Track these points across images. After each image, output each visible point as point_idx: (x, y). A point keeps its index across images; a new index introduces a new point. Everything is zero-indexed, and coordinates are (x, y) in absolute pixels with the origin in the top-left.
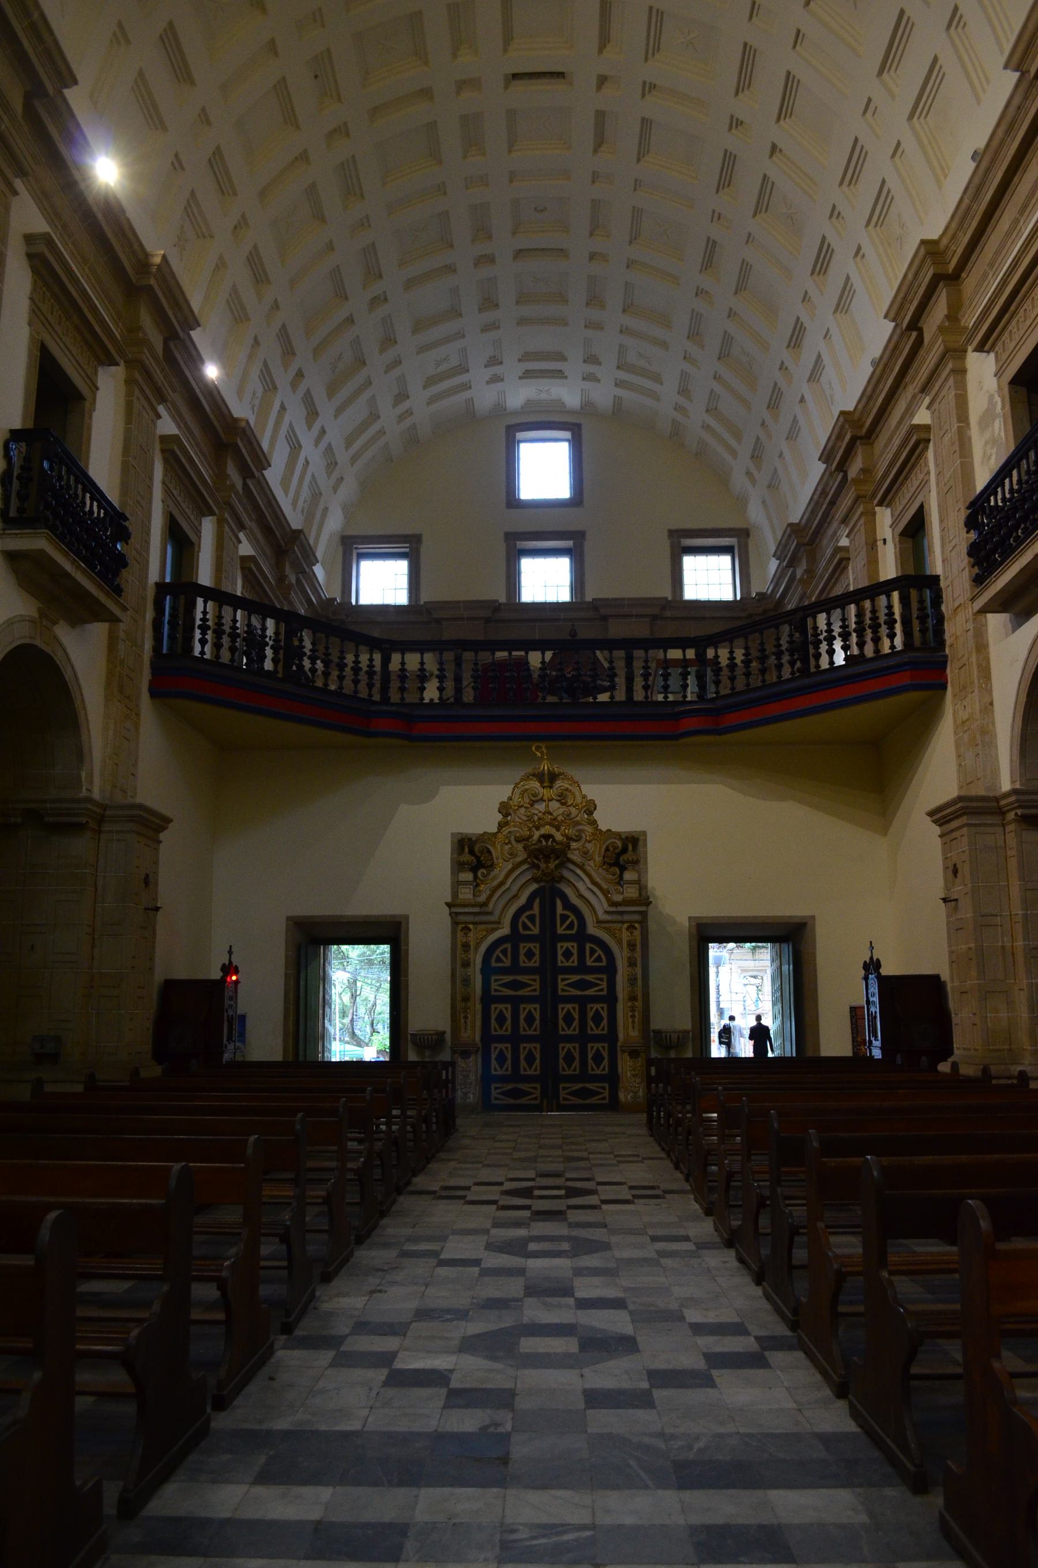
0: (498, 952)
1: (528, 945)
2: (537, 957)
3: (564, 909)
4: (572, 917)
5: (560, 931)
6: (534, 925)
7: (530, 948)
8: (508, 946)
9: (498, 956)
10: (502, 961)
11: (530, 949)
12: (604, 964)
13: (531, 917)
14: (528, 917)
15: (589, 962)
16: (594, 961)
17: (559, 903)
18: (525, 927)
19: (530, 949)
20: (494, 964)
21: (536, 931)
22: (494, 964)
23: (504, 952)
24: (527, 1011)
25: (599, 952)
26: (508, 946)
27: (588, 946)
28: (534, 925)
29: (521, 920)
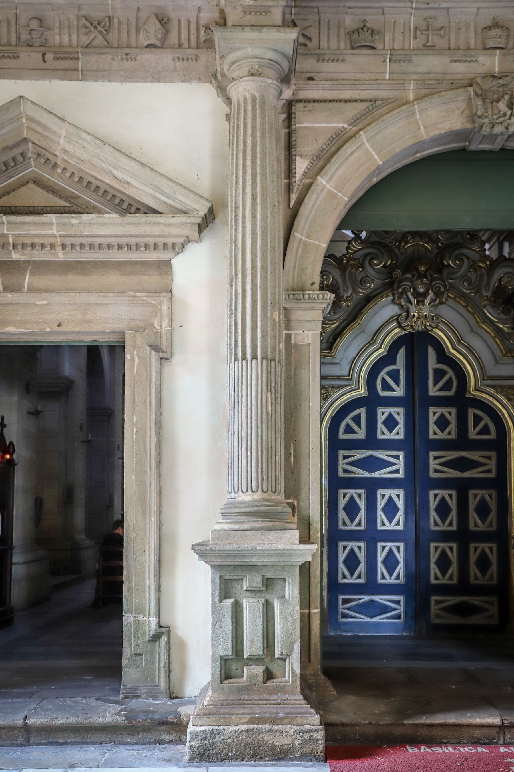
0: (348, 420)
1: (388, 411)
2: (401, 427)
3: (439, 361)
4: (451, 373)
5: (433, 391)
6: (398, 384)
7: (390, 415)
8: (362, 411)
9: (348, 425)
10: (354, 432)
11: (390, 415)
12: (493, 436)
14: (389, 373)
16: (479, 433)
18: (386, 386)
19: (390, 415)
20: (342, 436)
22: (342, 436)
23: (357, 420)
25: (486, 420)
26: (362, 411)
27: (471, 412)
28: (398, 384)
29: (379, 379)
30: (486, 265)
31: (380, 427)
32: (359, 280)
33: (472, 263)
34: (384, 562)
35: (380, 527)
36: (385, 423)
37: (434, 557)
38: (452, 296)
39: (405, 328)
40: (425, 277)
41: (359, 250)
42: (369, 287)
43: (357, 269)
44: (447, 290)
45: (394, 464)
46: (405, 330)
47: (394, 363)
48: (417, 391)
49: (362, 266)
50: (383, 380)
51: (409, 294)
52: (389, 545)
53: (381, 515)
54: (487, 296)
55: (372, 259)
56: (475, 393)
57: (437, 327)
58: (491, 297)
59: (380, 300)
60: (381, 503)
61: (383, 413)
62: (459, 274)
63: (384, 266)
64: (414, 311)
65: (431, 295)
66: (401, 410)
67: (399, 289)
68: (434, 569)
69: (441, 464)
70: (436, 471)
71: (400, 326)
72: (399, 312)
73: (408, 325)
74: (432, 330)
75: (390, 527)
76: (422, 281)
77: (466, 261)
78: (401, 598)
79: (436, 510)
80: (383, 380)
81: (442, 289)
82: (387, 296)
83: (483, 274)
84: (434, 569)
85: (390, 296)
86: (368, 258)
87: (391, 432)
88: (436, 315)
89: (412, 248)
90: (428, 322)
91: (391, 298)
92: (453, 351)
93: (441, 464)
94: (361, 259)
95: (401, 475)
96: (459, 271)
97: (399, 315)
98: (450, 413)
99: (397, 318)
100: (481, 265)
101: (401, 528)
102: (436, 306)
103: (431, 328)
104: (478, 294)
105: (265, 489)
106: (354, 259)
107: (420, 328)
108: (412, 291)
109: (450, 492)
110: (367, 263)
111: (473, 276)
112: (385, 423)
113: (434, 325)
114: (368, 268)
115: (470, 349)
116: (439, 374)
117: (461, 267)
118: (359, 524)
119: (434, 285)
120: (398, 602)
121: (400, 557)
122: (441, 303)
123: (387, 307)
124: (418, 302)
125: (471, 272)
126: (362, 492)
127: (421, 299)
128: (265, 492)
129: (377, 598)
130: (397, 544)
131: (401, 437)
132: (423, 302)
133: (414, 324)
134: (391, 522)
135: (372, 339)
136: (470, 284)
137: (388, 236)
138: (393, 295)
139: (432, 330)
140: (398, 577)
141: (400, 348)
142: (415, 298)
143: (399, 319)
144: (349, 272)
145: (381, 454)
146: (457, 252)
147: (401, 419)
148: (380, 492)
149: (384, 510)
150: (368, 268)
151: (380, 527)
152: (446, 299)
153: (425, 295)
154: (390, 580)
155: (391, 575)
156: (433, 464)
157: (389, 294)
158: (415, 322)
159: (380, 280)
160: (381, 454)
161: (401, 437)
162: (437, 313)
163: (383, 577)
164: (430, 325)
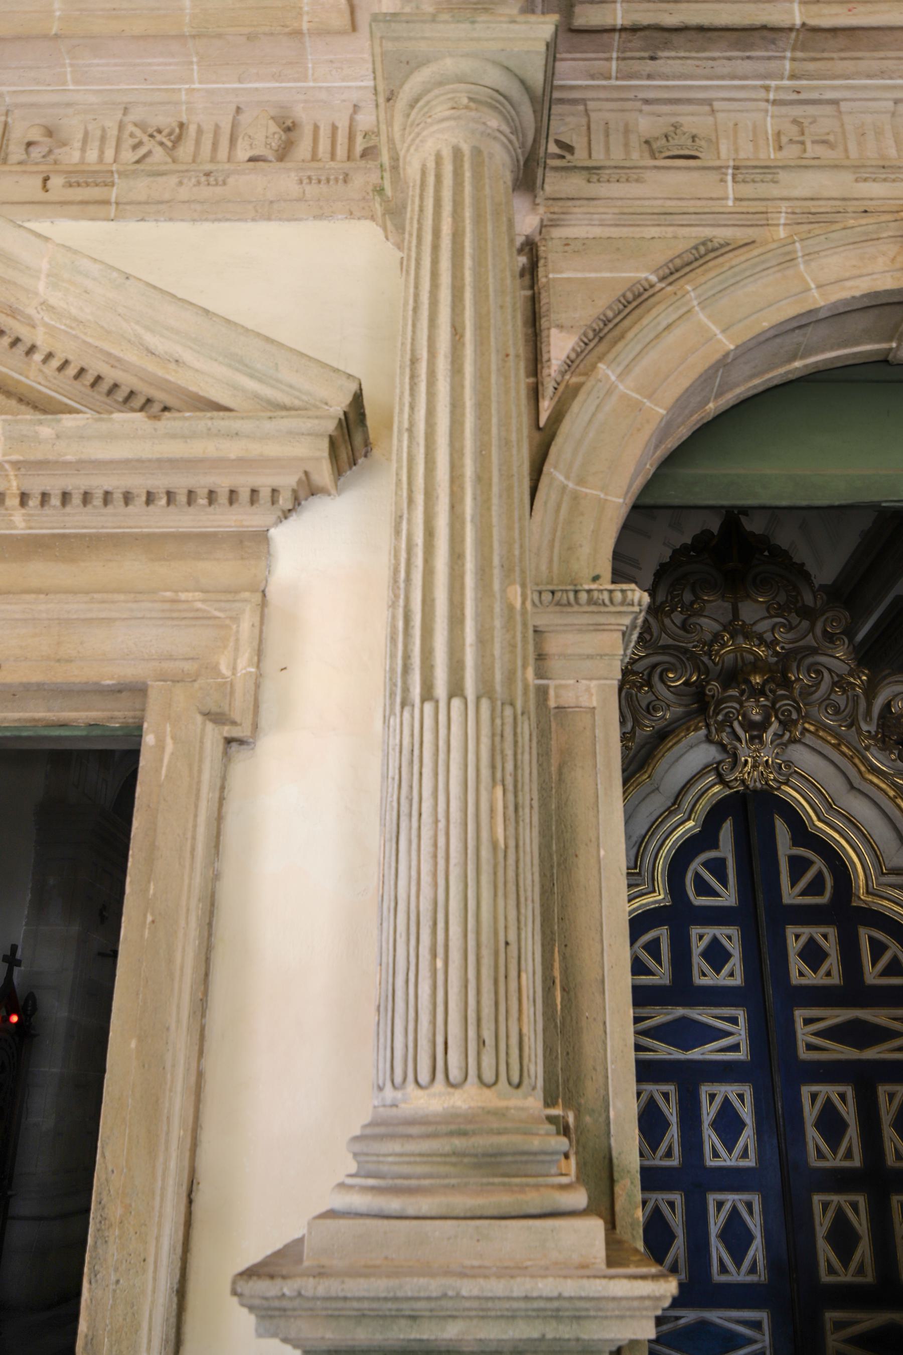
1: (710, 932)
2: (735, 963)
3: (795, 843)
4: (819, 864)
5: (790, 895)
8: (662, 933)
11: (715, 941)
13: (717, 868)
15: (872, 975)
17: (782, 831)
18: (703, 888)
19: (715, 941)
21: (728, 897)
24: (718, 1100)
27: (864, 934)
28: (724, 883)
29: (690, 876)
30: (862, 681)
31: (698, 961)
32: (644, 705)
33: (836, 679)
34: (723, 1235)
35: (710, 1162)
36: (705, 955)
37: (822, 1225)
38: (812, 728)
39: (731, 784)
40: (762, 693)
41: (641, 658)
42: (663, 717)
43: (640, 688)
44: (803, 717)
45: (729, 1034)
46: (731, 788)
47: (715, 846)
48: (760, 897)
49: (649, 683)
50: (698, 877)
51: (736, 725)
52: (731, 1198)
53: (710, 1137)
54: (869, 732)
55: (667, 670)
56: (869, 899)
57: (786, 783)
58: (877, 733)
59: (685, 736)
60: (709, 1112)
61: (701, 937)
62: (816, 696)
63: (686, 683)
64: (745, 753)
65: (775, 726)
66: (733, 931)
67: (718, 714)
68: (825, 1251)
69: (817, 1034)
70: (810, 1047)
71: (721, 780)
72: (719, 757)
73: (736, 779)
74: (779, 789)
75: (728, 1160)
76: (758, 701)
77: (826, 674)
78: (762, 1316)
79: (818, 1125)
80: (698, 877)
81: (794, 716)
82: (697, 729)
83: (857, 696)
84: (825, 1251)
85: (701, 728)
86: (659, 670)
87: (718, 972)
88: (784, 762)
89: (732, 655)
90: (771, 773)
91: (703, 732)
92: (820, 825)
93: (817, 1034)
94: (645, 673)
95: (742, 1055)
96: (815, 692)
97: (719, 763)
98: (825, 936)
99: (716, 768)
100: (852, 680)
101: (750, 1162)
102: (786, 745)
103: (778, 785)
104: (854, 729)
105: (489, 1076)
106: (636, 673)
107: (758, 784)
108: (740, 718)
109: (841, 1088)
110: (656, 679)
111: (839, 698)
112: (705, 955)
113: (781, 779)
114: (659, 687)
115: (849, 820)
116: (798, 866)
117: (820, 683)
118: (669, 1154)
119: (780, 707)
120: (756, 1325)
121: (755, 1224)
122: (793, 741)
123: (695, 749)
124: (752, 738)
125: (836, 692)
126: (670, 1088)
127: (755, 733)
128: (489, 1086)
129: (714, 1316)
130: (746, 1197)
131: (737, 981)
132: (760, 738)
133: (746, 776)
134: (730, 1150)
135: (674, 804)
136: (837, 711)
137: (689, 636)
138: (708, 726)
139: (779, 789)
140: (753, 1270)
141: (724, 820)
142: (746, 732)
143: (720, 769)
144: (627, 692)
145: (703, 1015)
146: (810, 660)
147: (734, 948)
148: (705, 1090)
149: (715, 1125)
150: (659, 687)
151: (710, 1162)
152: (802, 734)
153: (764, 726)
154: (738, 1276)
155: (738, 1263)
156: (803, 1034)
157: (700, 724)
158: (749, 773)
159: (680, 705)
160: (703, 1015)
161: (737, 981)
162: (785, 758)
163: (723, 1269)
164: (775, 780)
